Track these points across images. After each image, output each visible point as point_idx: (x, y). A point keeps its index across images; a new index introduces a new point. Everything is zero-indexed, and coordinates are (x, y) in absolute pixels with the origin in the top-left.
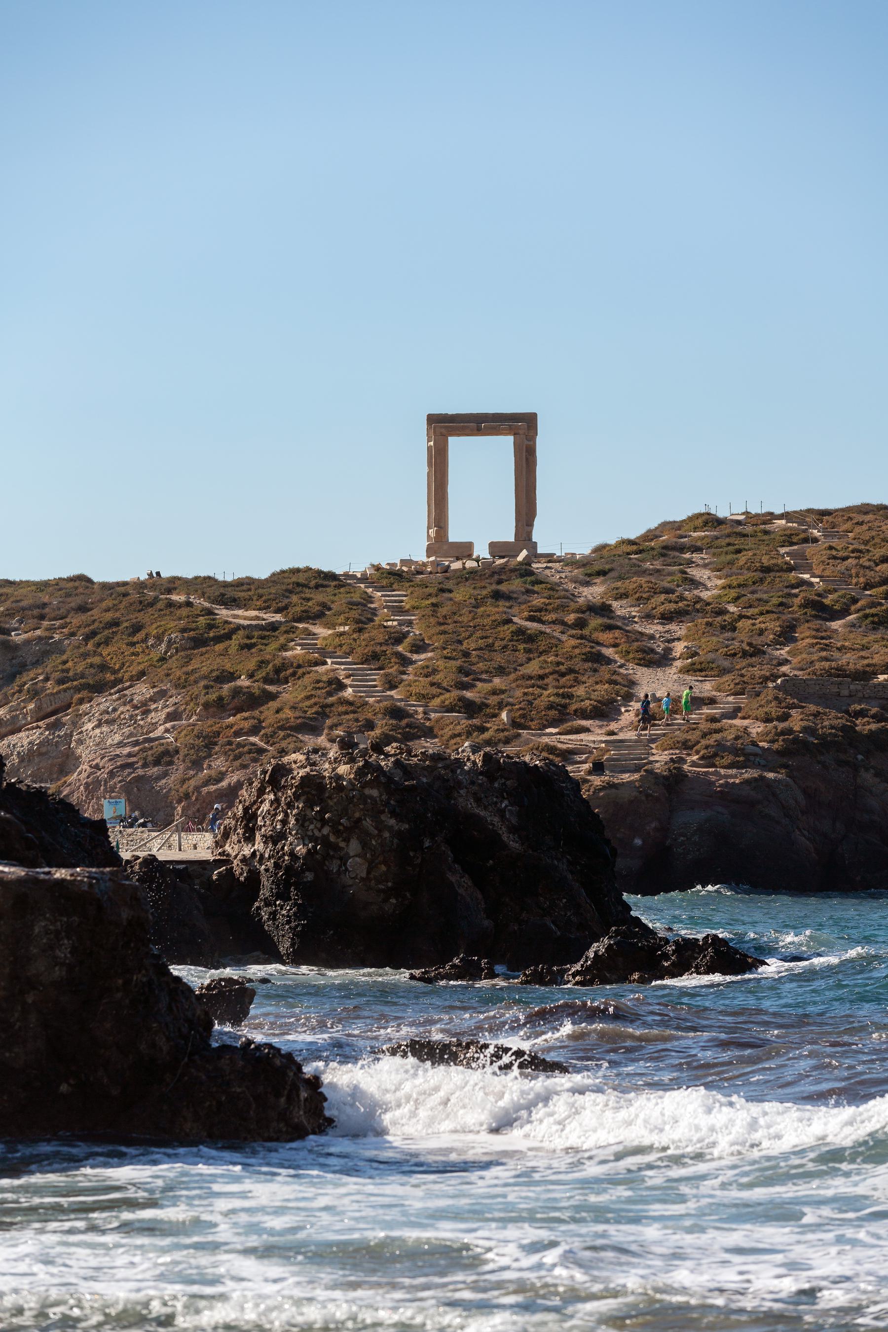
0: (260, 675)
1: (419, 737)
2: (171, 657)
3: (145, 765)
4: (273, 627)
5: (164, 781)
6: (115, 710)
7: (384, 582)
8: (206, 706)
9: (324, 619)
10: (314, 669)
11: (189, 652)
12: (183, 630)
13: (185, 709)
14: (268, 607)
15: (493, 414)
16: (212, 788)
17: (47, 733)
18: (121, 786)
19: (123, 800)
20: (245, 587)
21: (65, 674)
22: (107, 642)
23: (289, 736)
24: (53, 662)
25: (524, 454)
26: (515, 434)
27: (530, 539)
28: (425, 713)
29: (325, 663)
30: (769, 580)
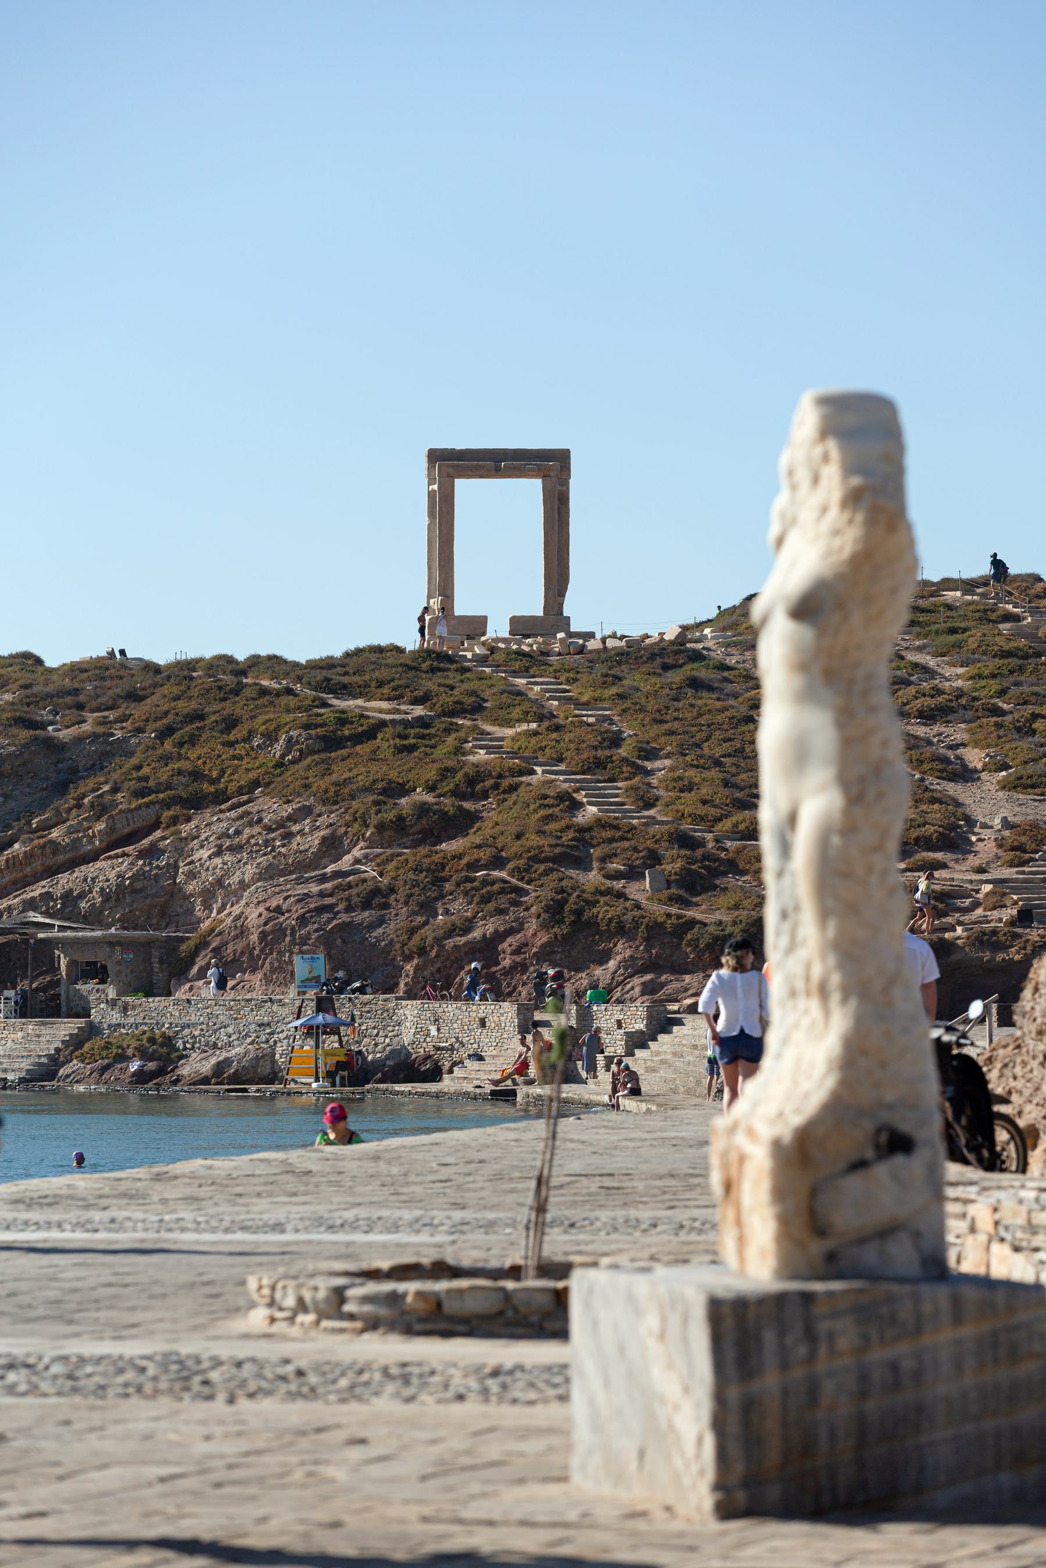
0: (447, 786)
1: (724, 874)
2: (293, 762)
3: (349, 909)
4: (423, 722)
5: (380, 931)
6: (238, 833)
7: (517, 665)
8: (381, 827)
9: (485, 713)
10: (523, 779)
11: (323, 755)
12: (307, 727)
13: (346, 833)
14: (400, 697)
15: (515, 451)
16: (461, 940)
17: (141, 862)
18: (319, 937)
19: (322, 956)
20: (339, 669)
21: (144, 784)
22: (192, 740)
23: (552, 870)
24: (119, 769)
25: (557, 503)
26: (544, 477)
27: (562, 613)
28: (717, 841)
29: (533, 772)
30: (1030, 668)
